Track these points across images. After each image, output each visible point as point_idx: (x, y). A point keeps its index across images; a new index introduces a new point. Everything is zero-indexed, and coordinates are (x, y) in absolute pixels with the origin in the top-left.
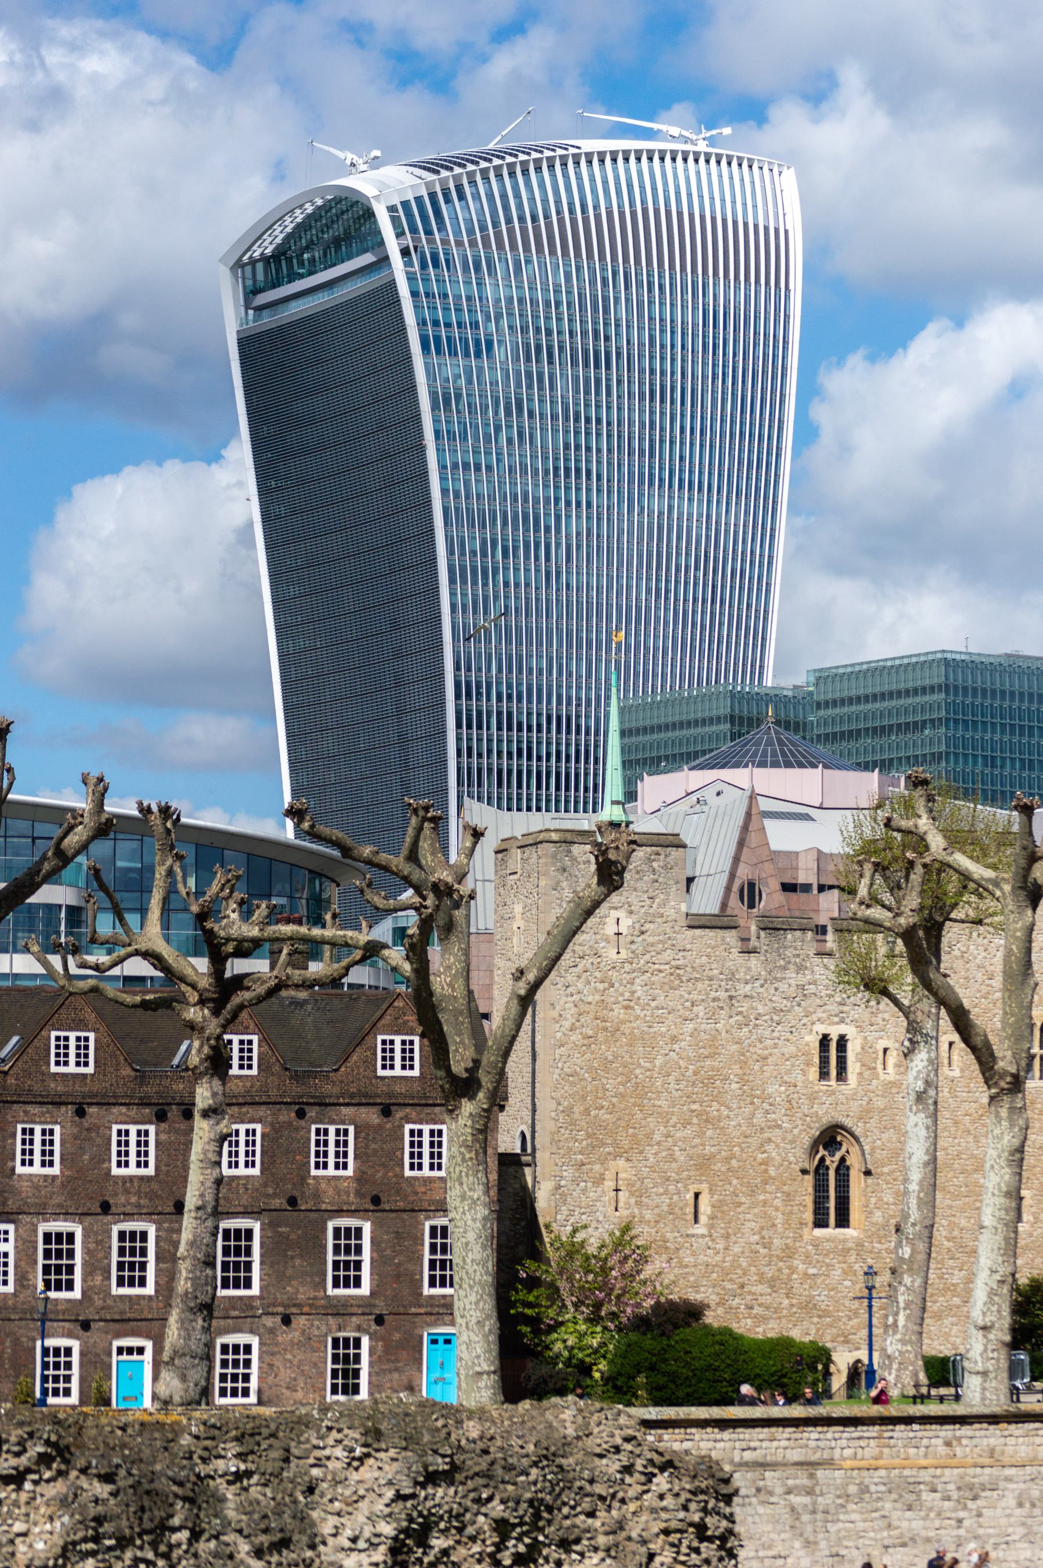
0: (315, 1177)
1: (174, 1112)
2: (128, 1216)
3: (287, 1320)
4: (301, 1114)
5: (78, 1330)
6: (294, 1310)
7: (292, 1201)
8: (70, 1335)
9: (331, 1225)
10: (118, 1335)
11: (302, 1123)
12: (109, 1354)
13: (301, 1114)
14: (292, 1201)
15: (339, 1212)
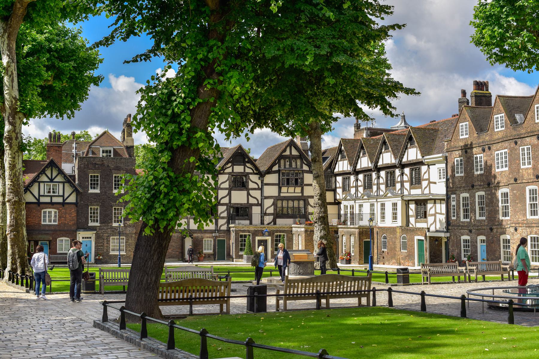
0: (522, 169)
1: (487, 149)
2: (479, 190)
3: (516, 230)
4: (516, 143)
5: (470, 234)
6: (517, 225)
7: (516, 180)
8: (468, 235)
9: (528, 188)
10: (479, 235)
11: (517, 147)
12: (477, 242)
13: (516, 143)
14: (516, 180)
15: (528, 183)
